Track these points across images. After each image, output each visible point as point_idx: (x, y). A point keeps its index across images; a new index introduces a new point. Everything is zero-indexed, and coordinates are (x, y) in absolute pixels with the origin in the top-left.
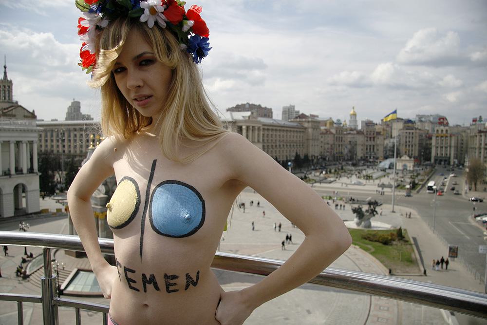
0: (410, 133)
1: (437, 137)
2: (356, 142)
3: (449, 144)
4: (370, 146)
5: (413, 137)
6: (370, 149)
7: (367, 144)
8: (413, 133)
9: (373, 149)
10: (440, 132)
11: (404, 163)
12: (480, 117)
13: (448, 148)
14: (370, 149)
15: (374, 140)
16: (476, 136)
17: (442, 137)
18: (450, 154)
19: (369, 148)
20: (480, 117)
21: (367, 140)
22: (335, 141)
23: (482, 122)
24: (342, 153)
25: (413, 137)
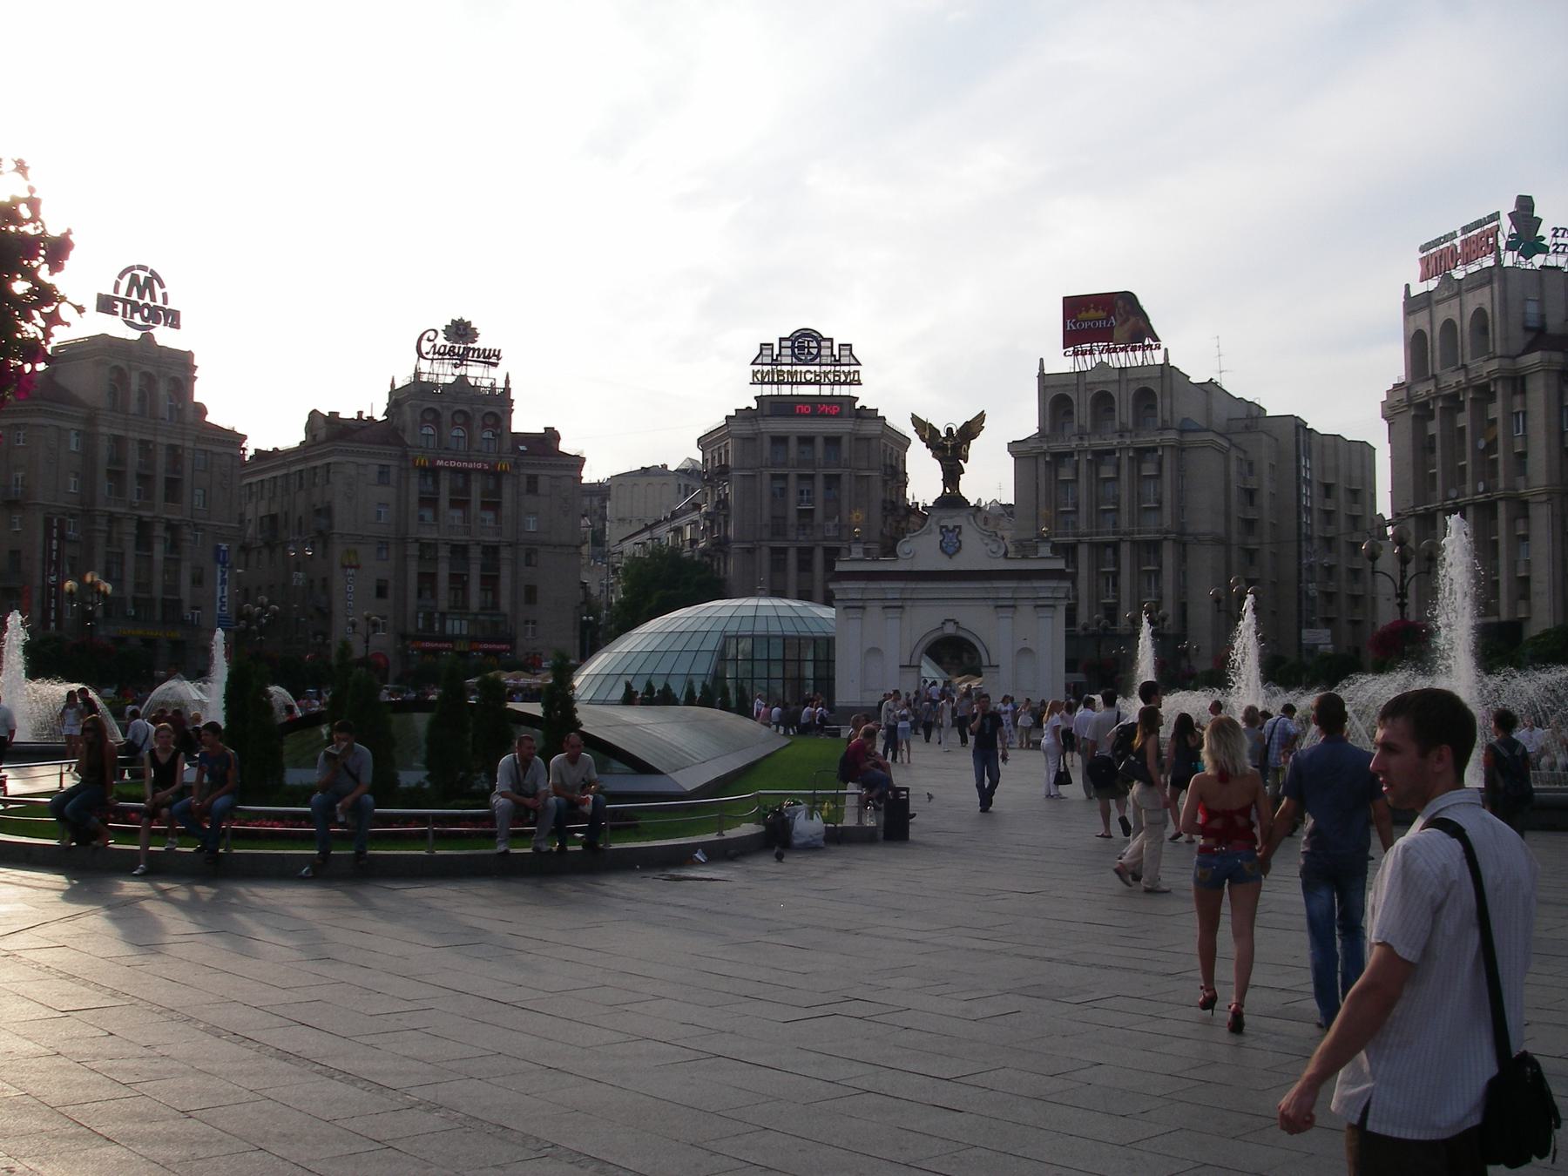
0: (806, 440)
1: (1059, 458)
2: (326, 512)
3: (1167, 522)
4: (459, 551)
5: (832, 481)
6: (459, 582)
7: (429, 535)
8: (833, 441)
9: (490, 582)
10: (1083, 413)
11: (927, 619)
12: (1525, 210)
13: (1168, 556)
14: (459, 582)
15: (492, 505)
16: (1517, 383)
17: (1100, 456)
18: (1183, 609)
19: (443, 571)
20: (1525, 210)
21: (429, 501)
22: (103, 485)
23: (1538, 260)
24: (172, 607)
25: (832, 481)
